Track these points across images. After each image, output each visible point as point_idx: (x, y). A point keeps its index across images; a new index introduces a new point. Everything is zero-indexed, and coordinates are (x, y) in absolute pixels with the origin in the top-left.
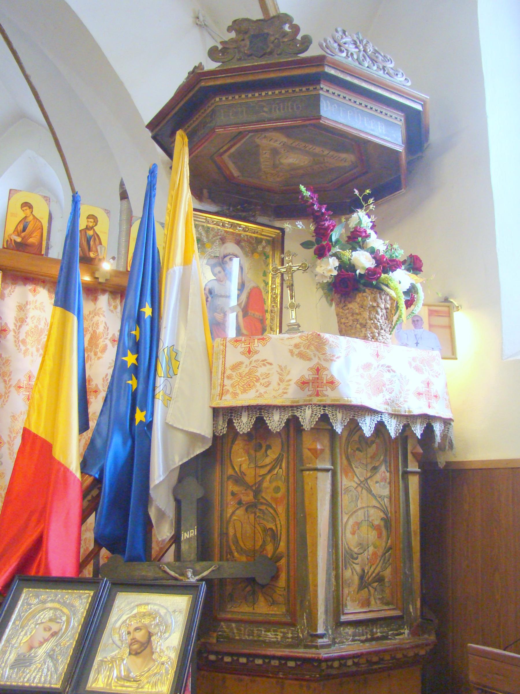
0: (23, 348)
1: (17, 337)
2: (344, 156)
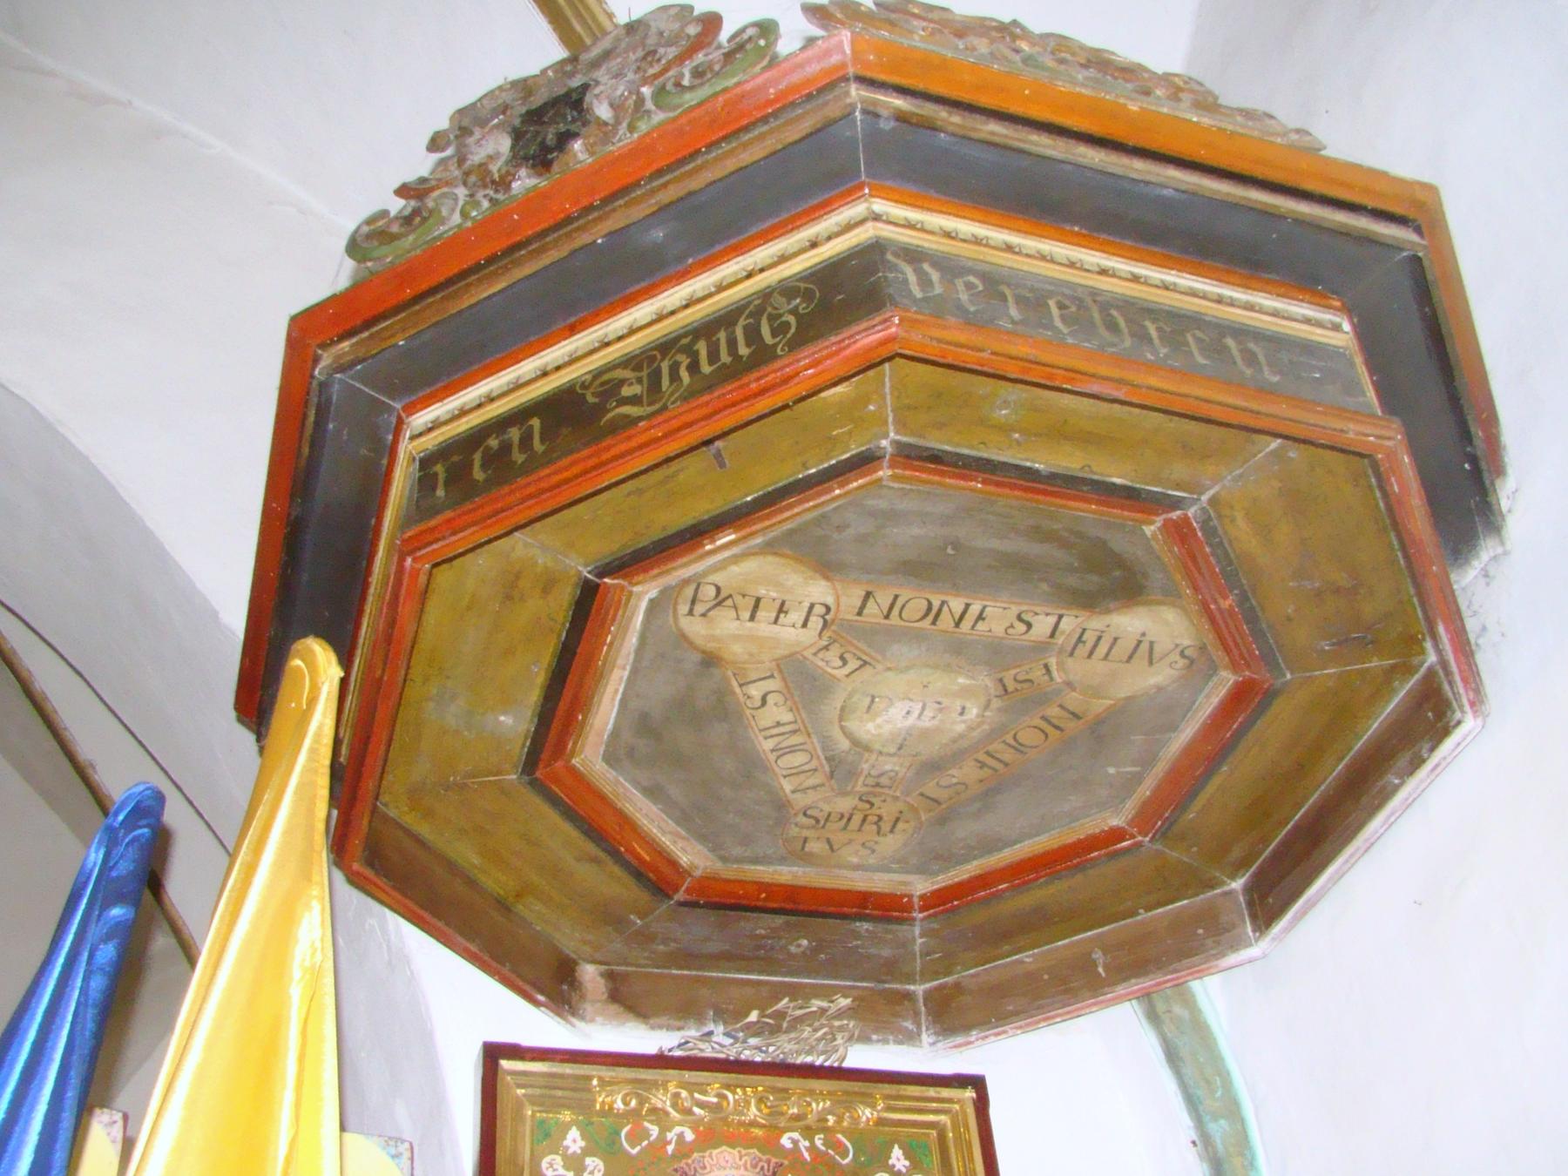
2: (1130, 623)
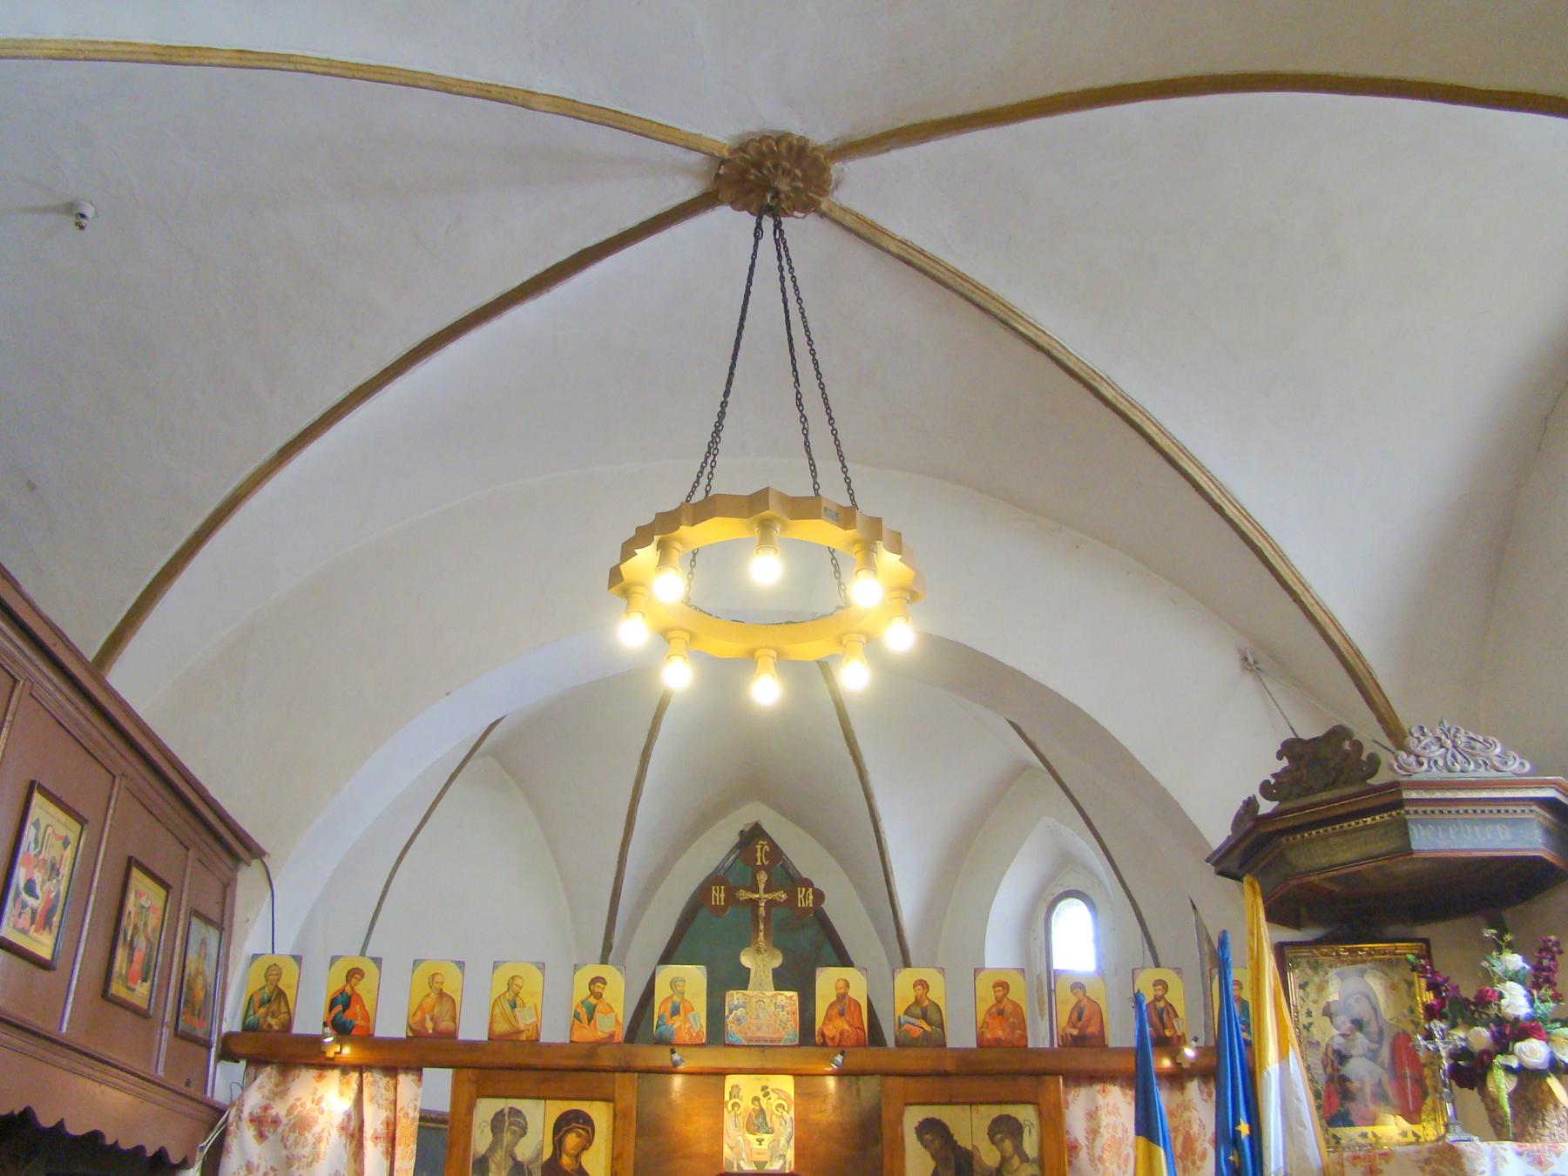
0: (1100, 1166)
1: (1092, 1160)
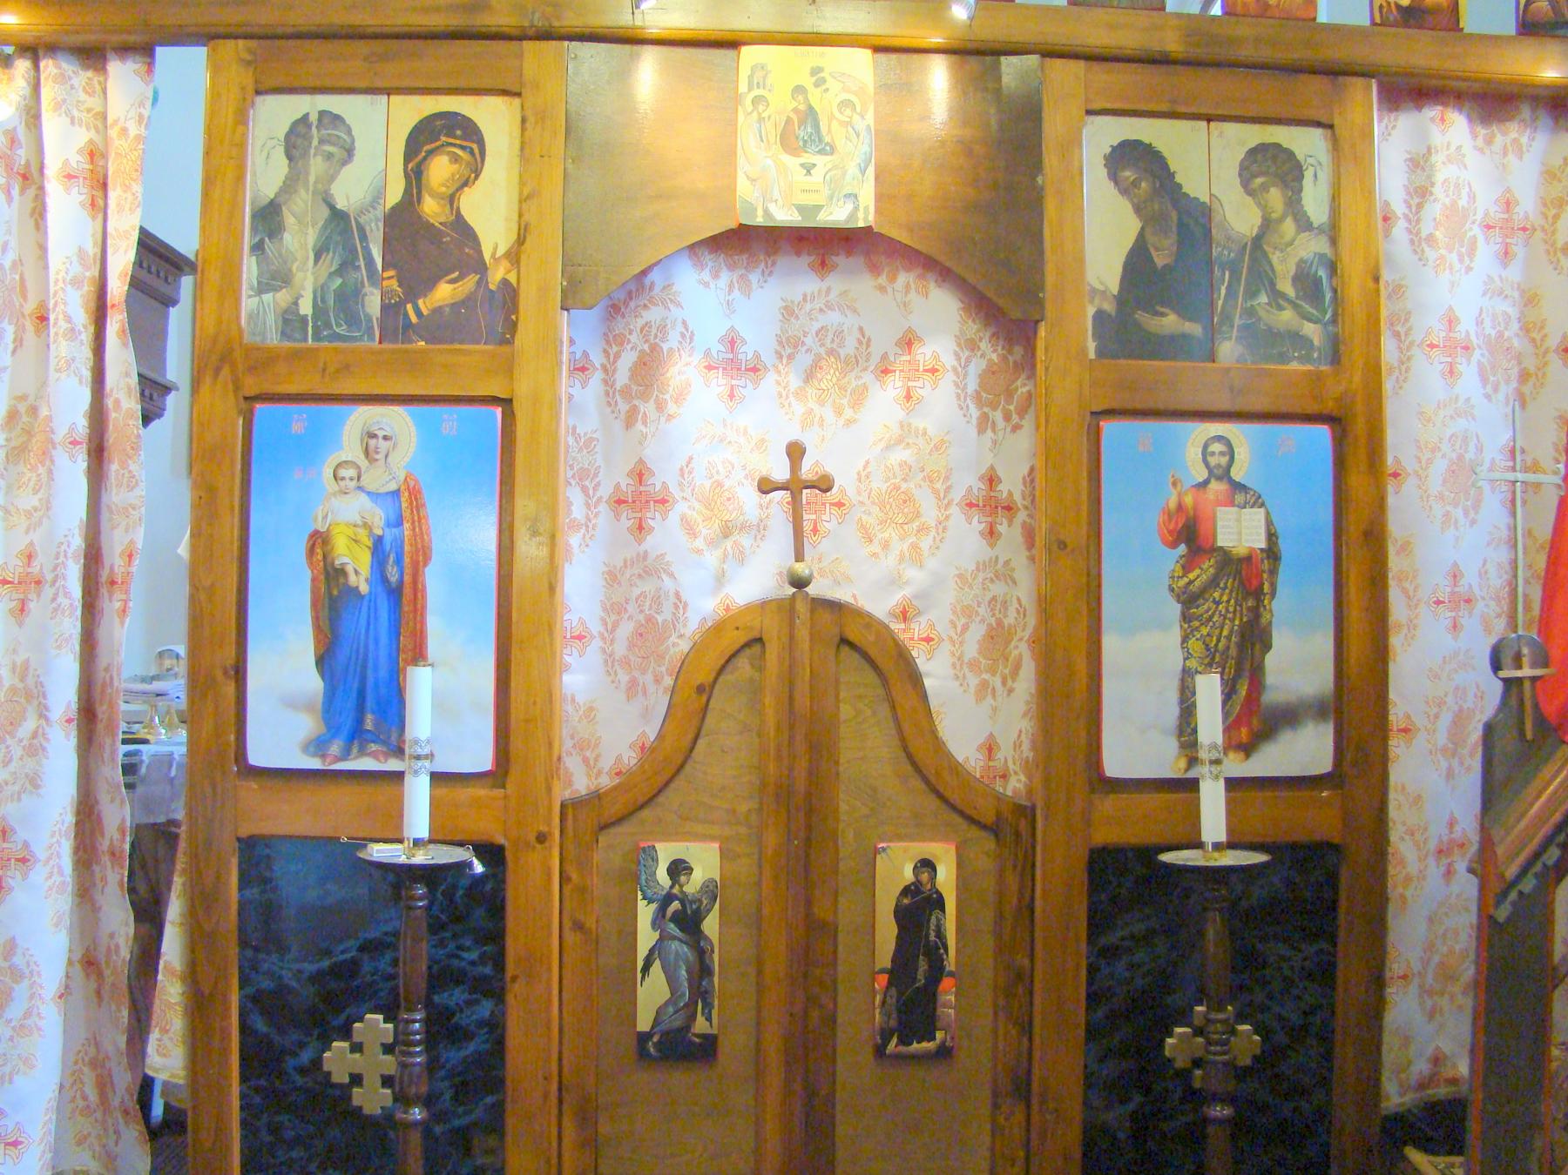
0: (1430, 254)
